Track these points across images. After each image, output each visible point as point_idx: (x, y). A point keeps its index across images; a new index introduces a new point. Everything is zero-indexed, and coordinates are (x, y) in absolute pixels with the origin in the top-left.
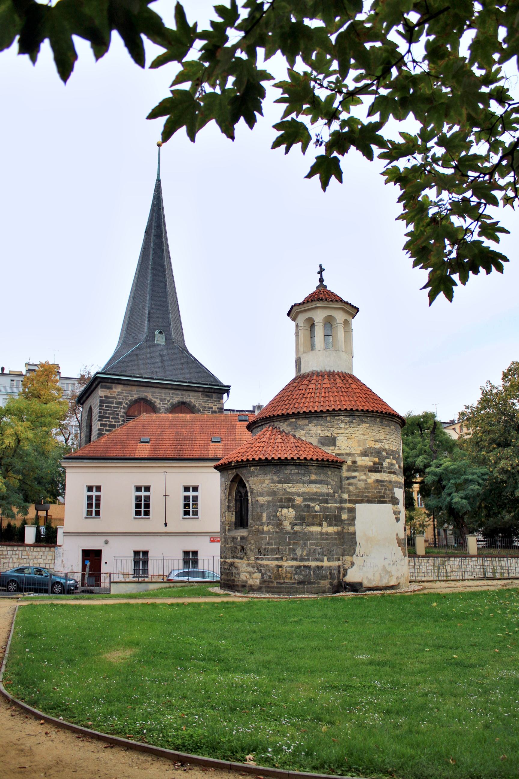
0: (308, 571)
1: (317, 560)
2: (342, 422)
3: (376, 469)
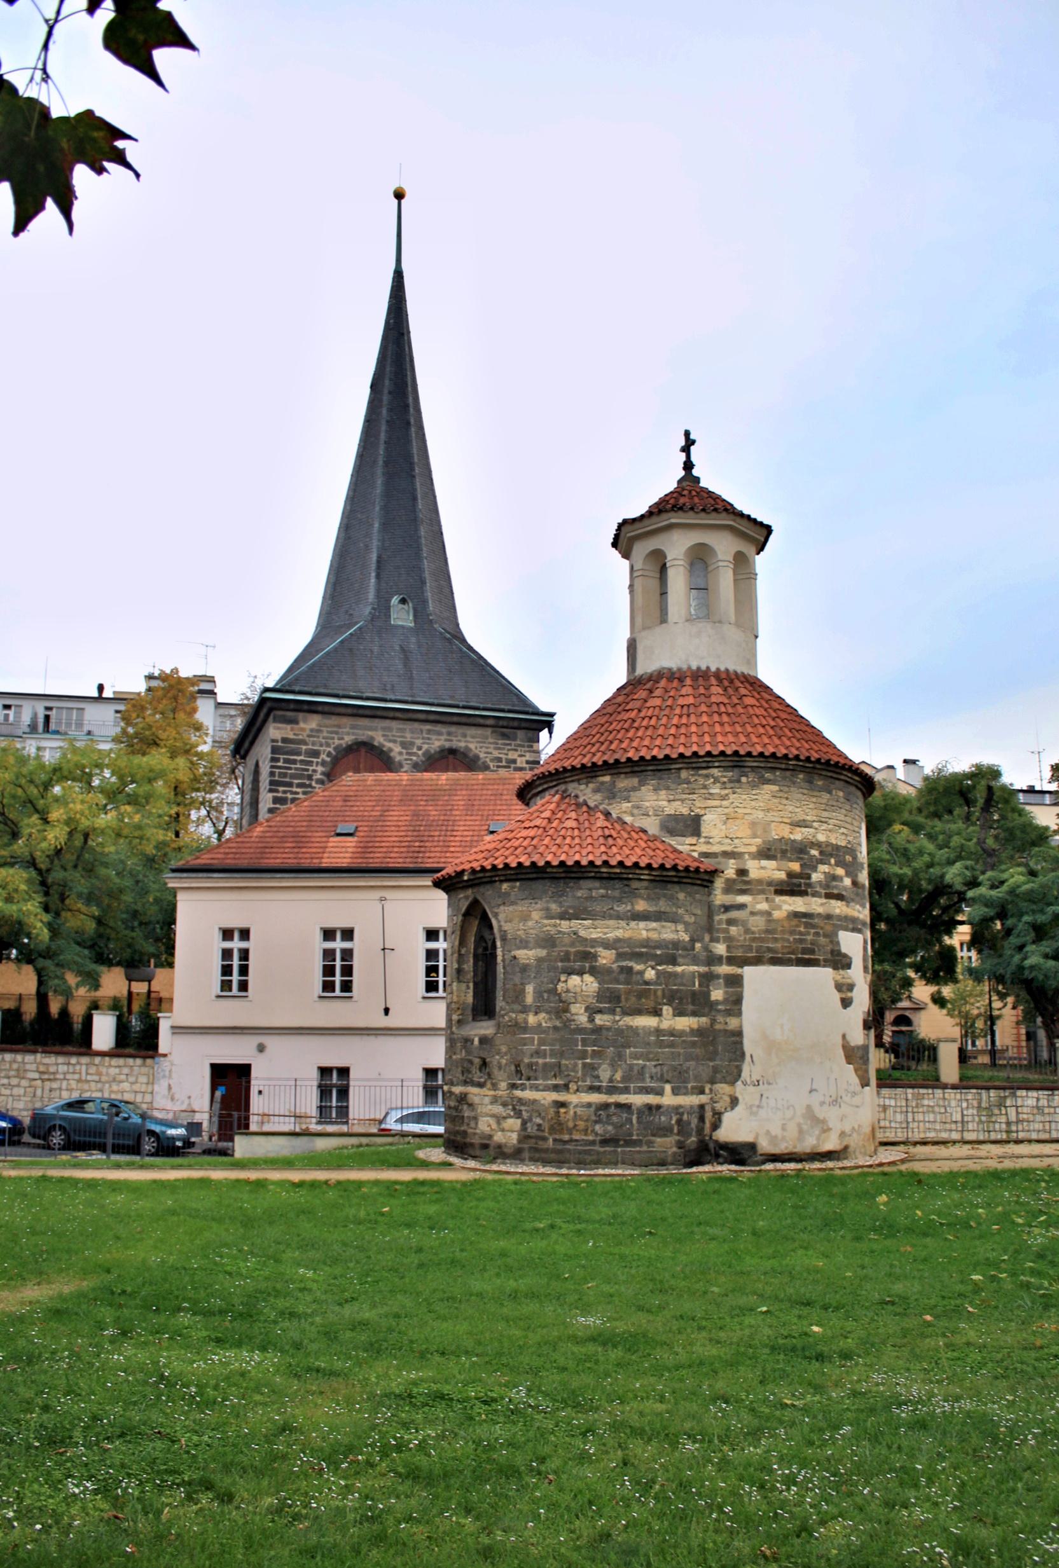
0: (625, 1115)
1: (647, 1091)
2: (716, 780)
3: (793, 887)
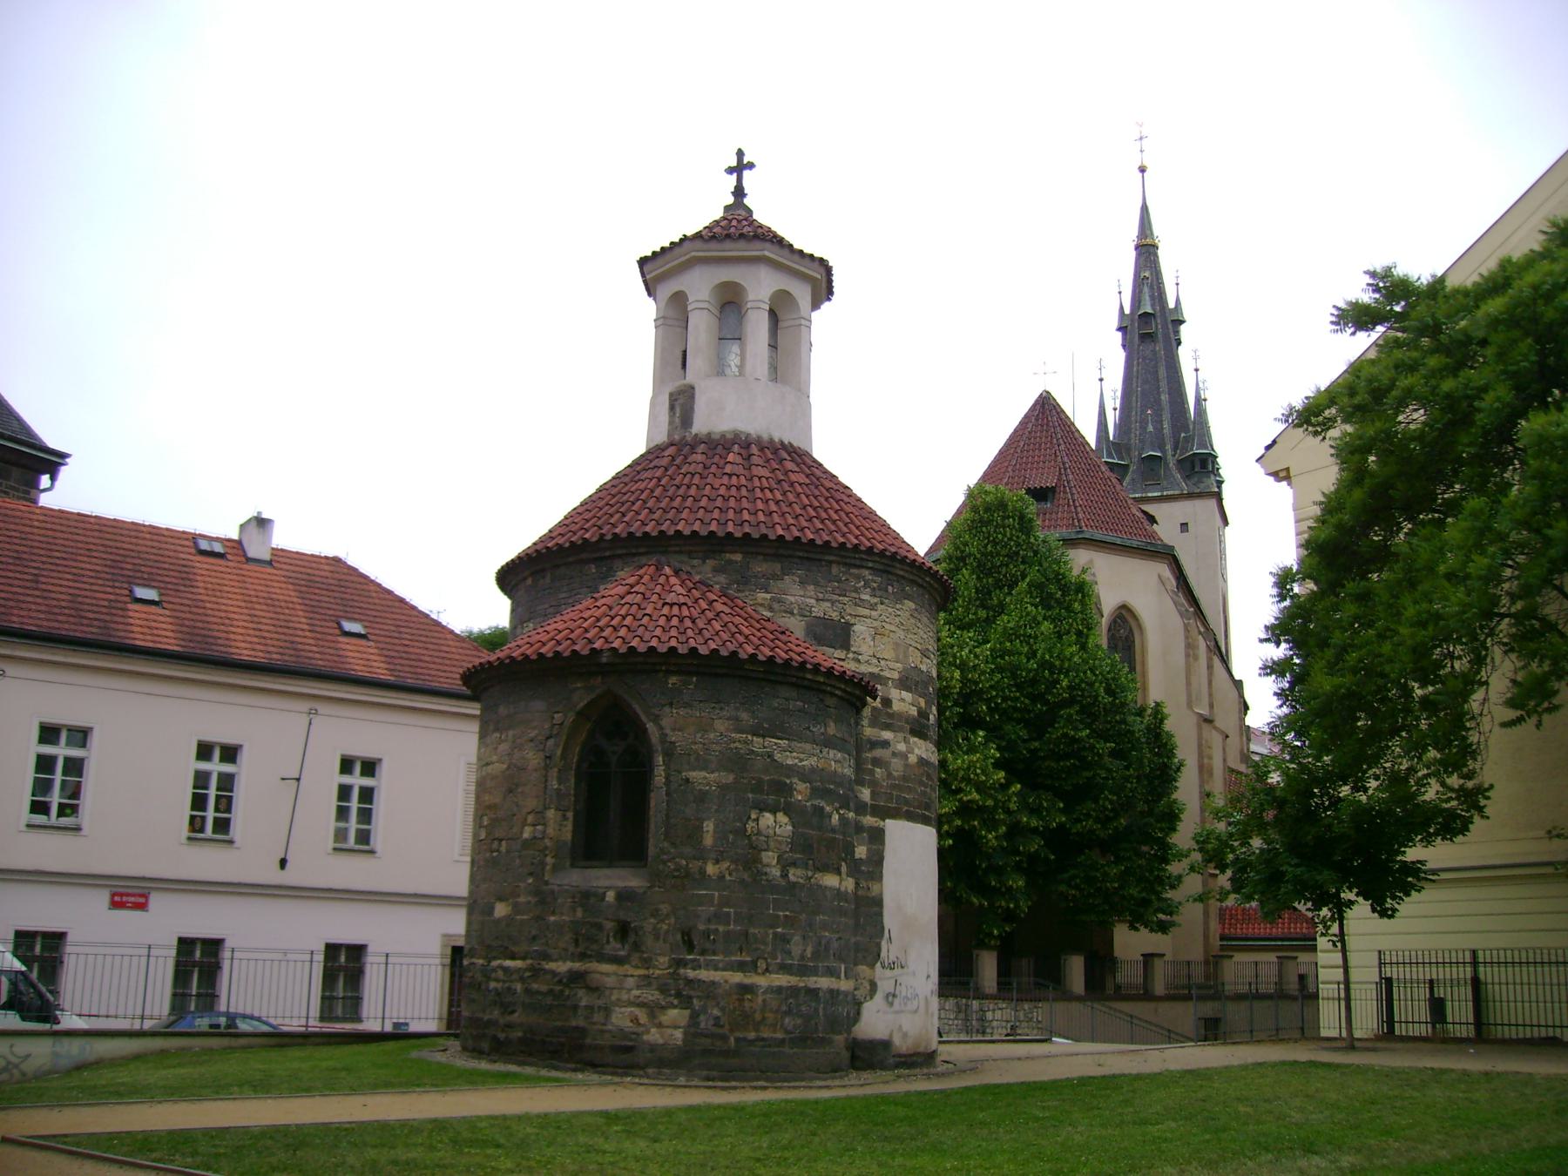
1: (832, 973)
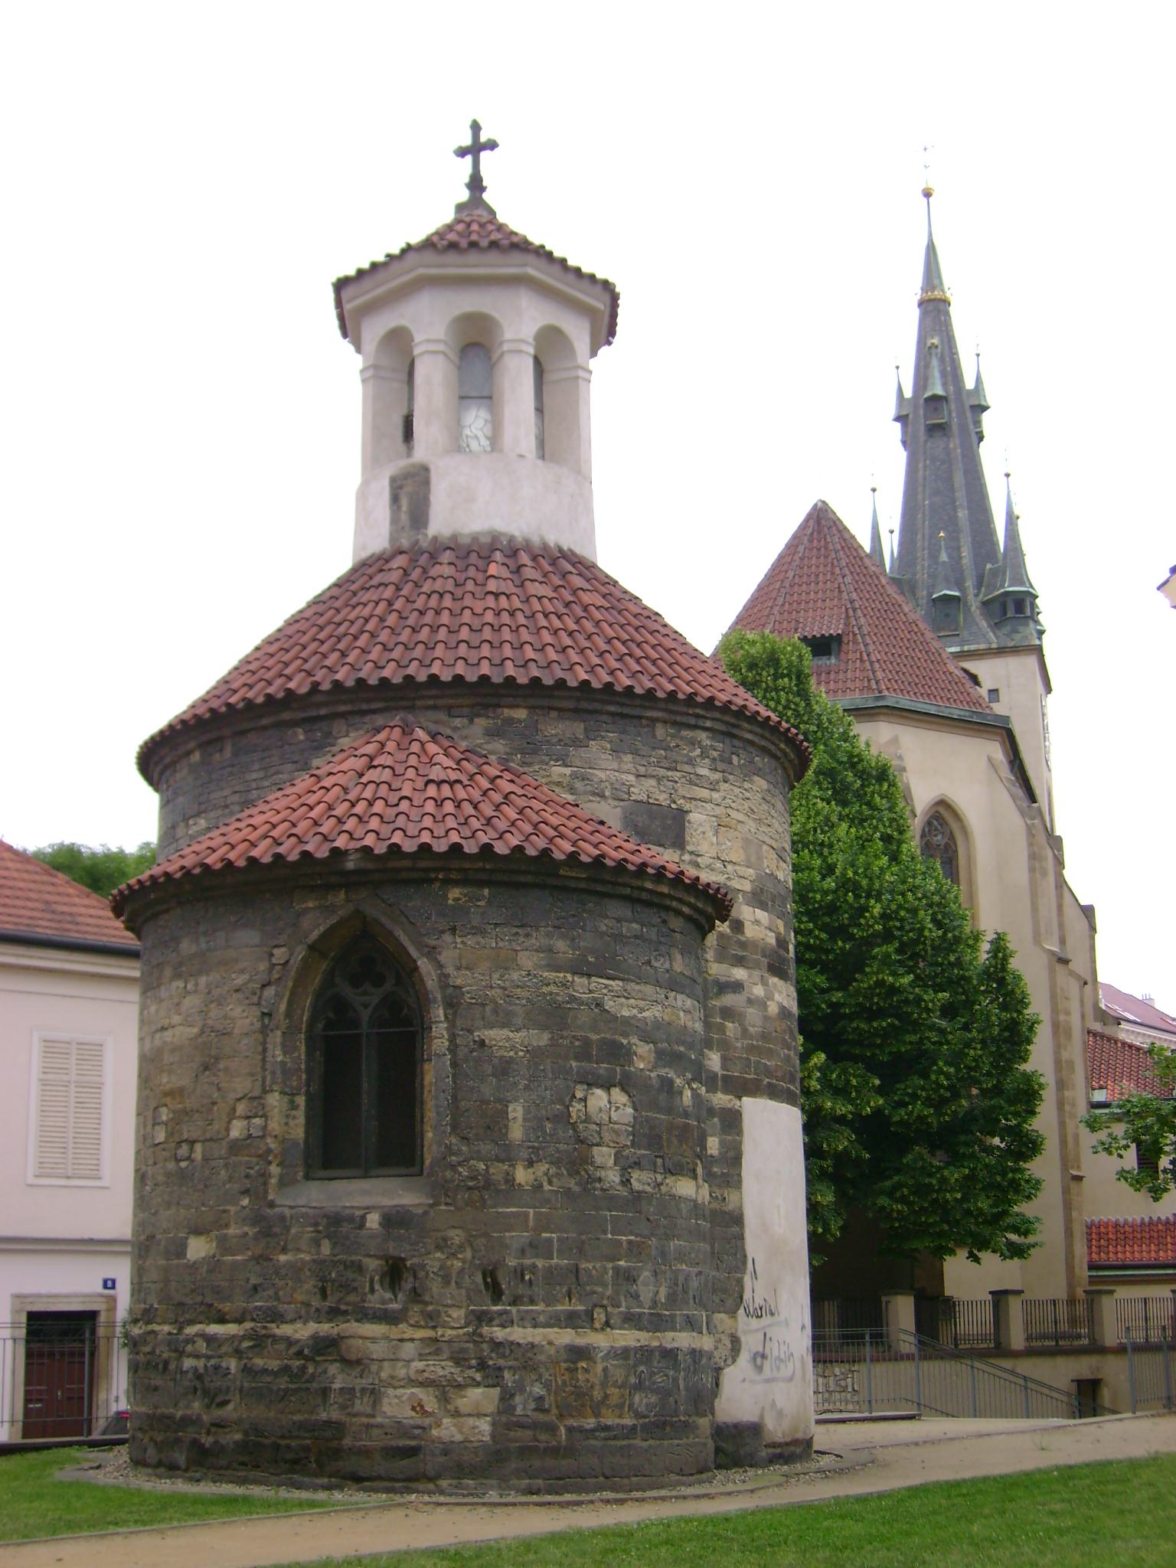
1: (691, 1324)
2: (704, 755)
